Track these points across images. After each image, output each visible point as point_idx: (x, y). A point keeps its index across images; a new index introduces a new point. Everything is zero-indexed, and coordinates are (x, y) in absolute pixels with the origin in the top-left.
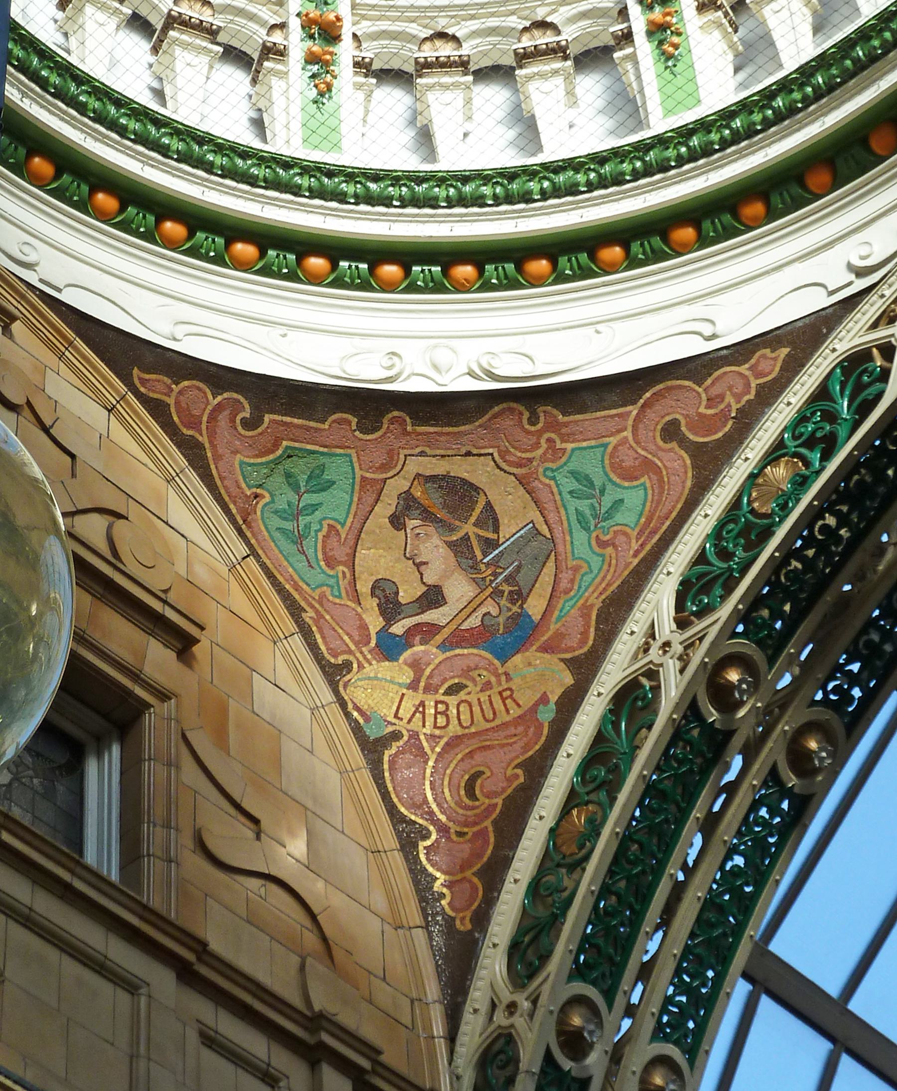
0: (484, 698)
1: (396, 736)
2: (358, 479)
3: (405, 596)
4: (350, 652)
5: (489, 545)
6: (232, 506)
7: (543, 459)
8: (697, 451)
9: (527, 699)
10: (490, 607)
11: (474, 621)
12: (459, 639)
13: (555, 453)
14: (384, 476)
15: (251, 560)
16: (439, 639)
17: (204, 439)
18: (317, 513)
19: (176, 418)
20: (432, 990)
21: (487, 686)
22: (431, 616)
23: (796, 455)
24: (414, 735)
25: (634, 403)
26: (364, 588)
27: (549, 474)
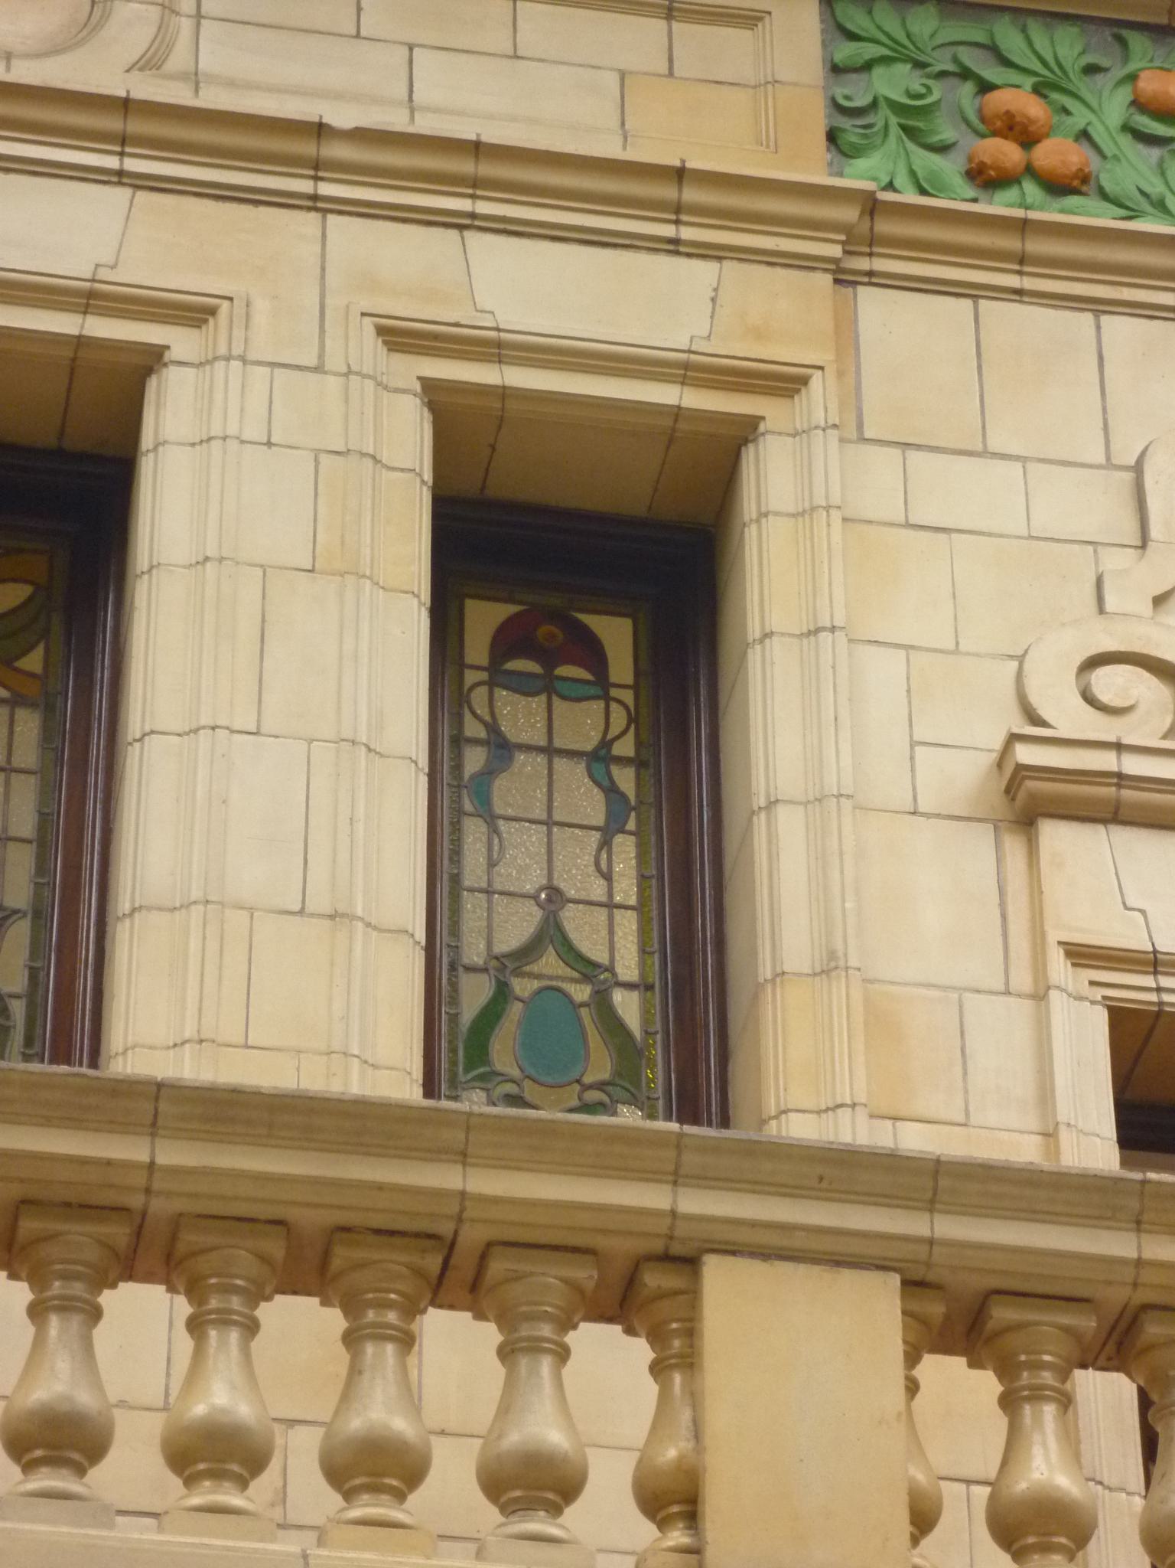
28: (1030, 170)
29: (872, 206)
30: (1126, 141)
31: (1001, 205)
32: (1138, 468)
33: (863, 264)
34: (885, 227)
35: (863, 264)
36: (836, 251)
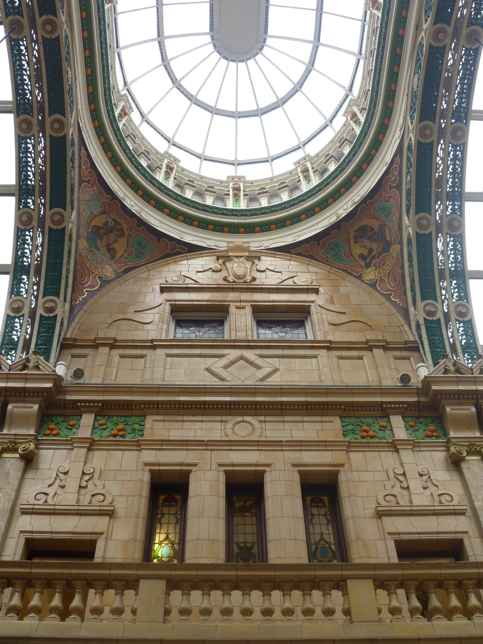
0: (389, 262)
1: (377, 280)
3: (366, 253)
4: (361, 271)
5: (374, 234)
7: (373, 211)
8: (396, 187)
9: (395, 257)
10: (382, 245)
11: (380, 249)
12: (380, 254)
13: (374, 208)
15: (333, 268)
16: (376, 257)
17: (312, 253)
20: (403, 322)
21: (389, 259)
22: (373, 254)
24: (381, 278)
25: (381, 188)
26: (357, 258)
28: (368, 436)
29: (349, 442)
30: (379, 431)
31: (365, 440)
32: (387, 471)
33: (349, 449)
34: (351, 445)
35: (349, 449)
36: (346, 448)
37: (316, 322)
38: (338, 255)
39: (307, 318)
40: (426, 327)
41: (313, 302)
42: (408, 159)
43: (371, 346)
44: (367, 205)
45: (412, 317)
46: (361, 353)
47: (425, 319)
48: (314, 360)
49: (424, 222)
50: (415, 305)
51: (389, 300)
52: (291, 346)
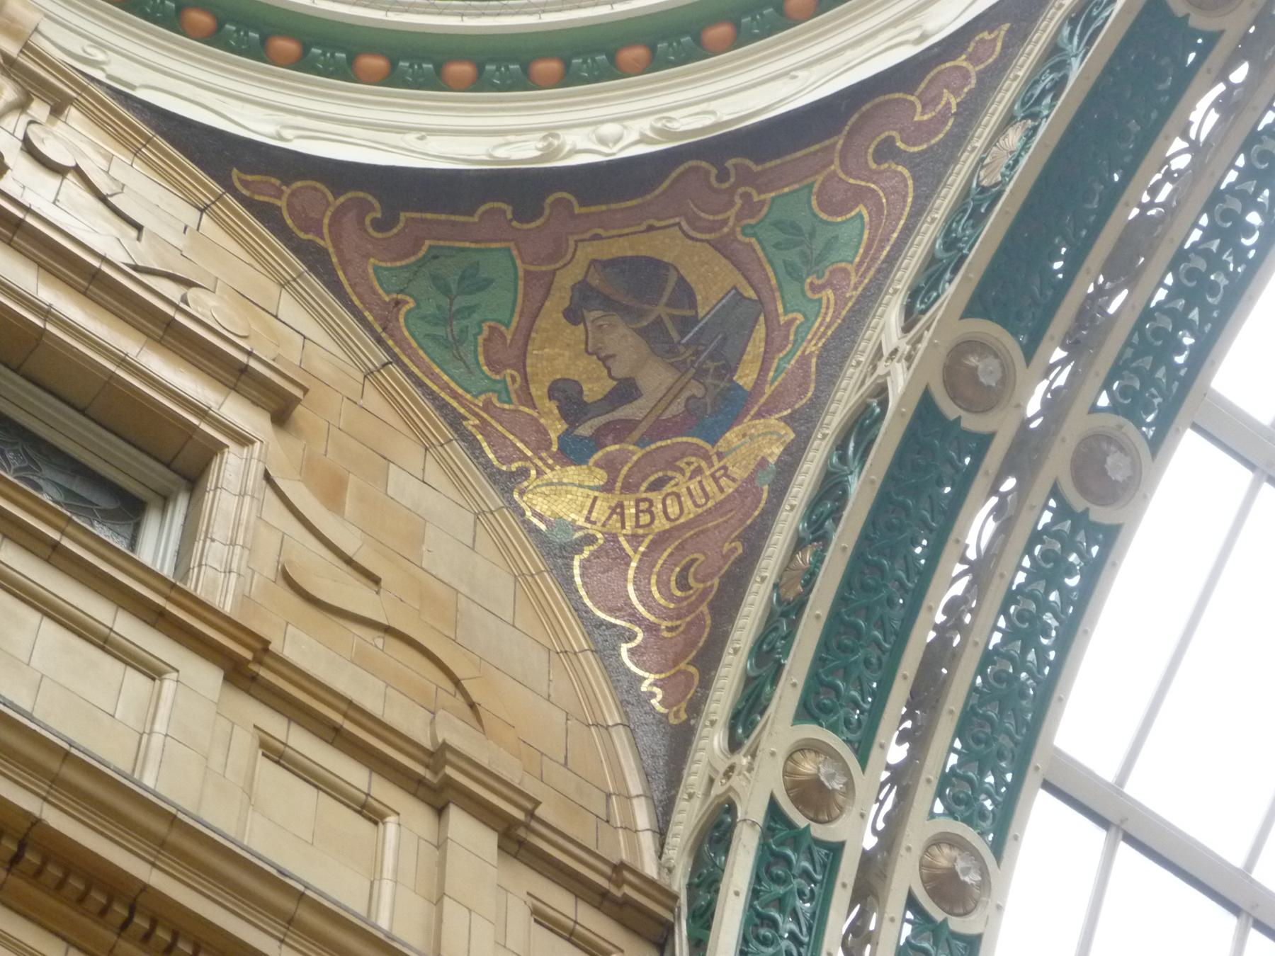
0: (693, 485)
1: (590, 539)
2: (521, 274)
4: (526, 458)
5: (685, 324)
6: (367, 314)
7: (739, 218)
9: (739, 473)
10: (696, 390)
11: (677, 408)
12: (661, 429)
13: (750, 208)
14: (552, 267)
15: (394, 368)
16: (636, 435)
17: (326, 243)
18: (475, 315)
19: (289, 222)
21: (698, 471)
22: (625, 412)
23: (1023, 118)
24: (612, 538)
25: (838, 132)
26: (539, 391)
27: (749, 231)
37: (220, 530)
38: (457, 325)
39: (165, 500)
40: (764, 847)
41: (244, 440)
42: (1055, 57)
43: (449, 783)
44: (723, 176)
45: (694, 777)
46: (385, 792)
47: (774, 809)
48: (136, 681)
49: (986, 369)
50: (750, 726)
51: (606, 655)
52: (55, 546)
